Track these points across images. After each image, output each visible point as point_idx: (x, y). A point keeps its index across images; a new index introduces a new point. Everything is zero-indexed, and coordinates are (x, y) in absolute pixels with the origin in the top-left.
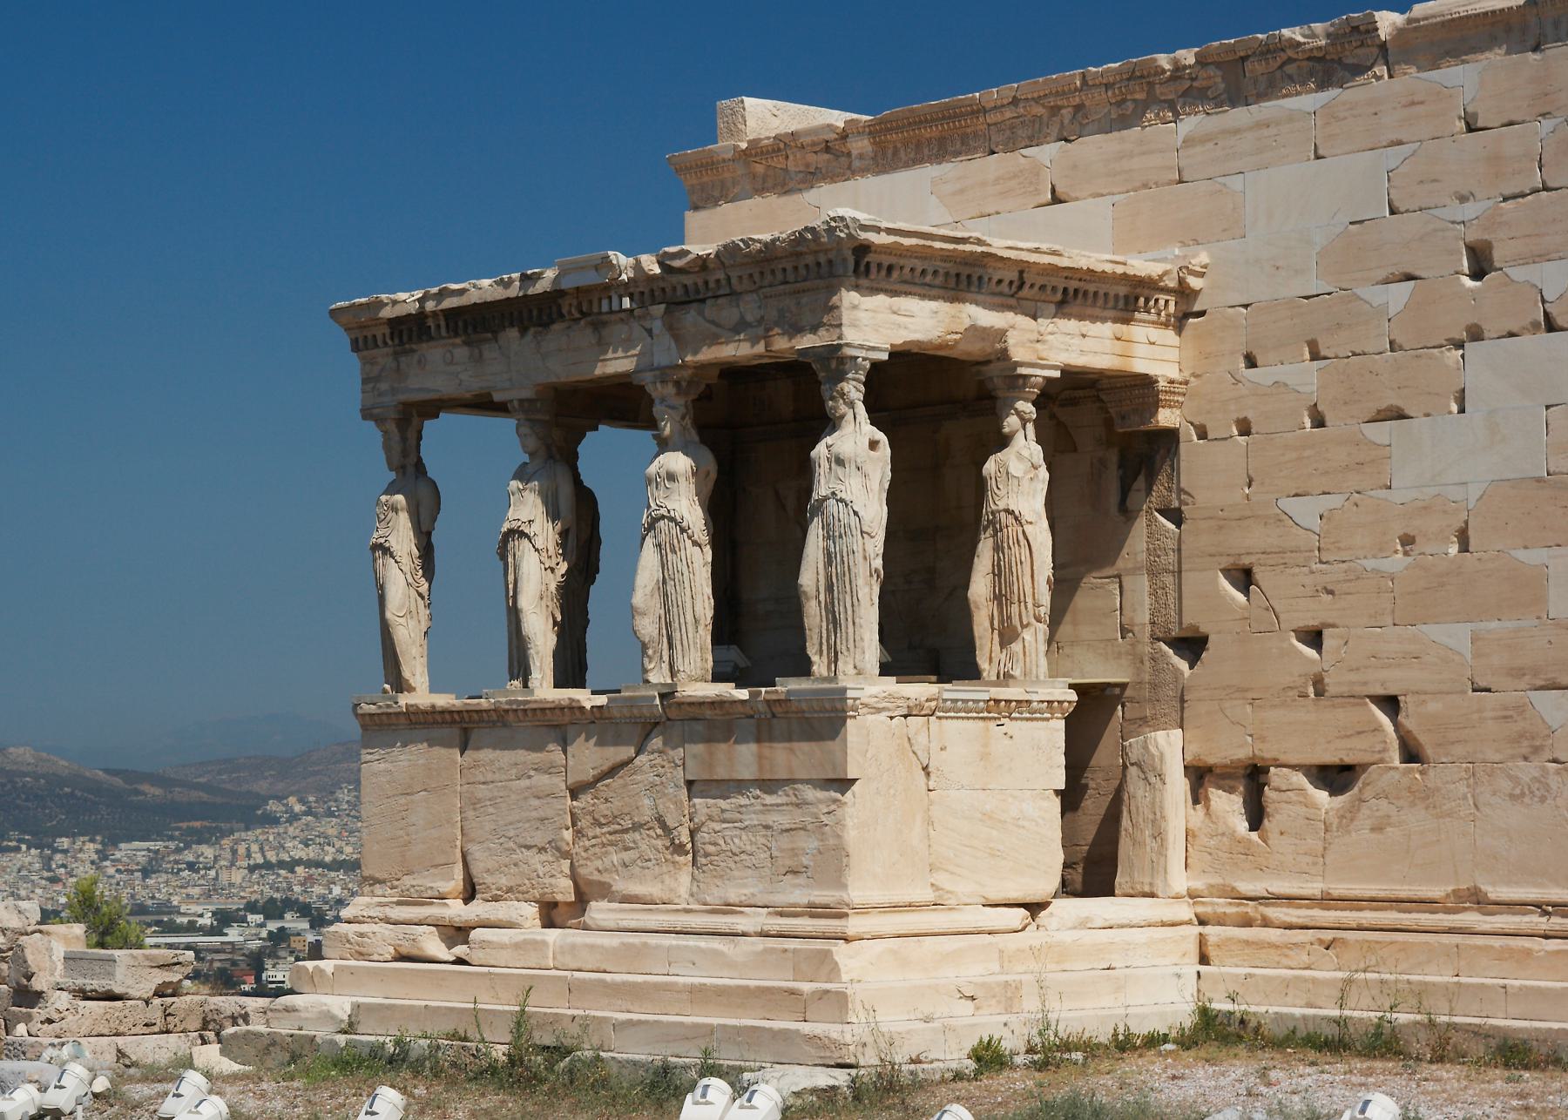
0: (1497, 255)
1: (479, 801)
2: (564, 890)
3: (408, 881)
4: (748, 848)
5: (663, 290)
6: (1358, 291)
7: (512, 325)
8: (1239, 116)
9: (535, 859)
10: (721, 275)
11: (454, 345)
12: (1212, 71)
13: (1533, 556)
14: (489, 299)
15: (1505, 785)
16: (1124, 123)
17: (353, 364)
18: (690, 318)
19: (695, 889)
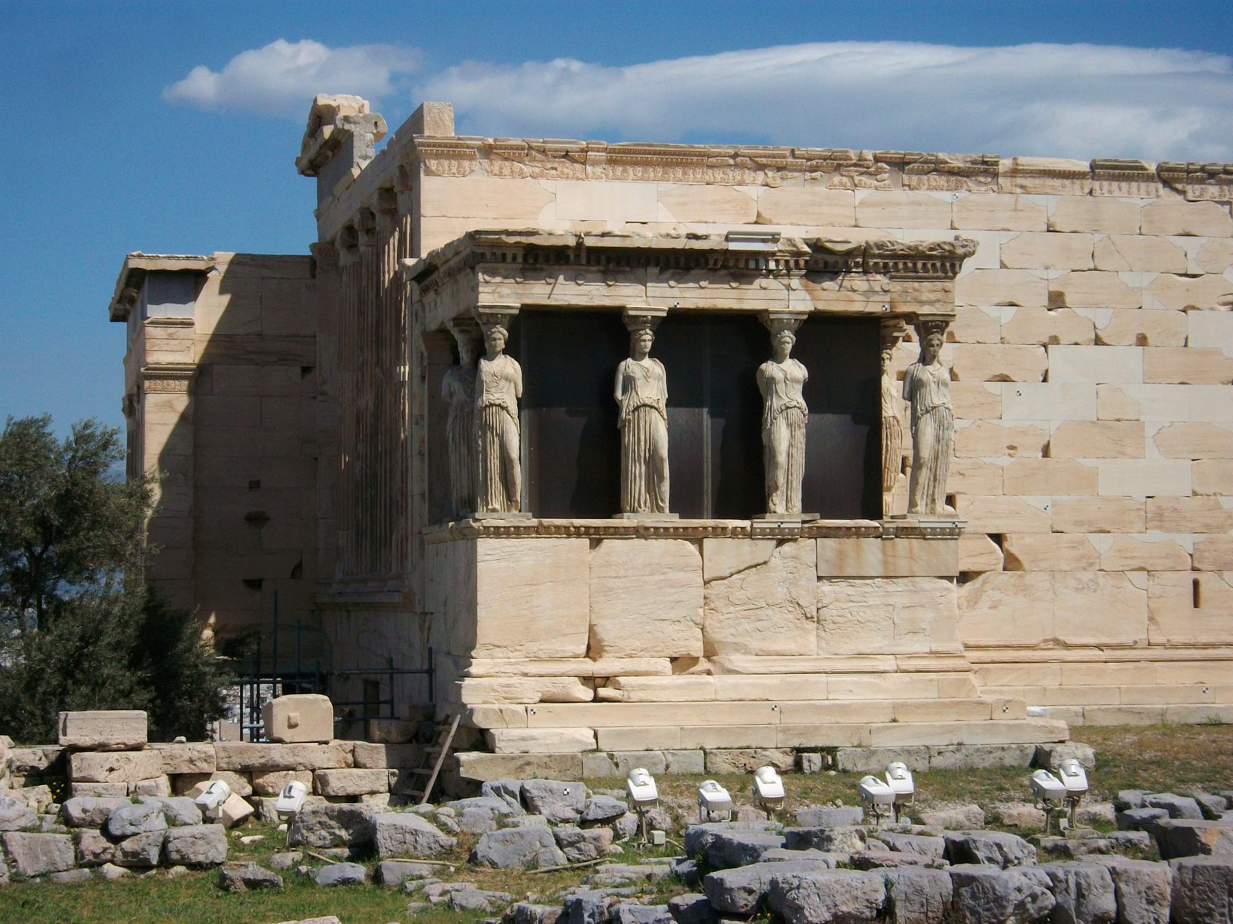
1: (611, 589)
2: (697, 648)
3: (534, 647)
4: (872, 618)
5: (806, 261)
6: (981, 308)
7: (657, 265)
8: (899, 194)
9: (670, 629)
10: (859, 260)
11: (587, 271)
12: (884, 165)
13: (1090, 462)
14: (654, 246)
15: (1073, 583)
19: (823, 644)
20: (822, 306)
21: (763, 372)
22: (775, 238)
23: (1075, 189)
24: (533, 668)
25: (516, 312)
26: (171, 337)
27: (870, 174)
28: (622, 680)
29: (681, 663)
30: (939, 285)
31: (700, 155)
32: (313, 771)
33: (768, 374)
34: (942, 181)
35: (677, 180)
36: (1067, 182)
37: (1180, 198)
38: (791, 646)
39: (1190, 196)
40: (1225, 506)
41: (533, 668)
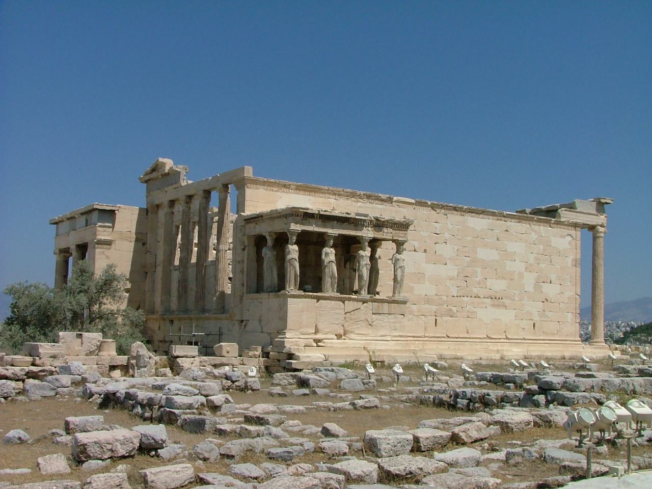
2: (342, 332)
3: (302, 330)
8: (368, 205)
13: (412, 285)
14: (338, 215)
15: (407, 319)
20: (376, 236)
21: (359, 254)
22: (367, 216)
23: (411, 207)
25: (300, 232)
26: (104, 231)
27: (361, 199)
28: (324, 340)
29: (339, 337)
30: (404, 232)
31: (319, 189)
32: (233, 366)
33: (361, 254)
34: (379, 202)
35: (313, 196)
36: (409, 206)
37: (435, 212)
38: (365, 333)
39: (438, 212)
40: (443, 299)
41: (302, 336)
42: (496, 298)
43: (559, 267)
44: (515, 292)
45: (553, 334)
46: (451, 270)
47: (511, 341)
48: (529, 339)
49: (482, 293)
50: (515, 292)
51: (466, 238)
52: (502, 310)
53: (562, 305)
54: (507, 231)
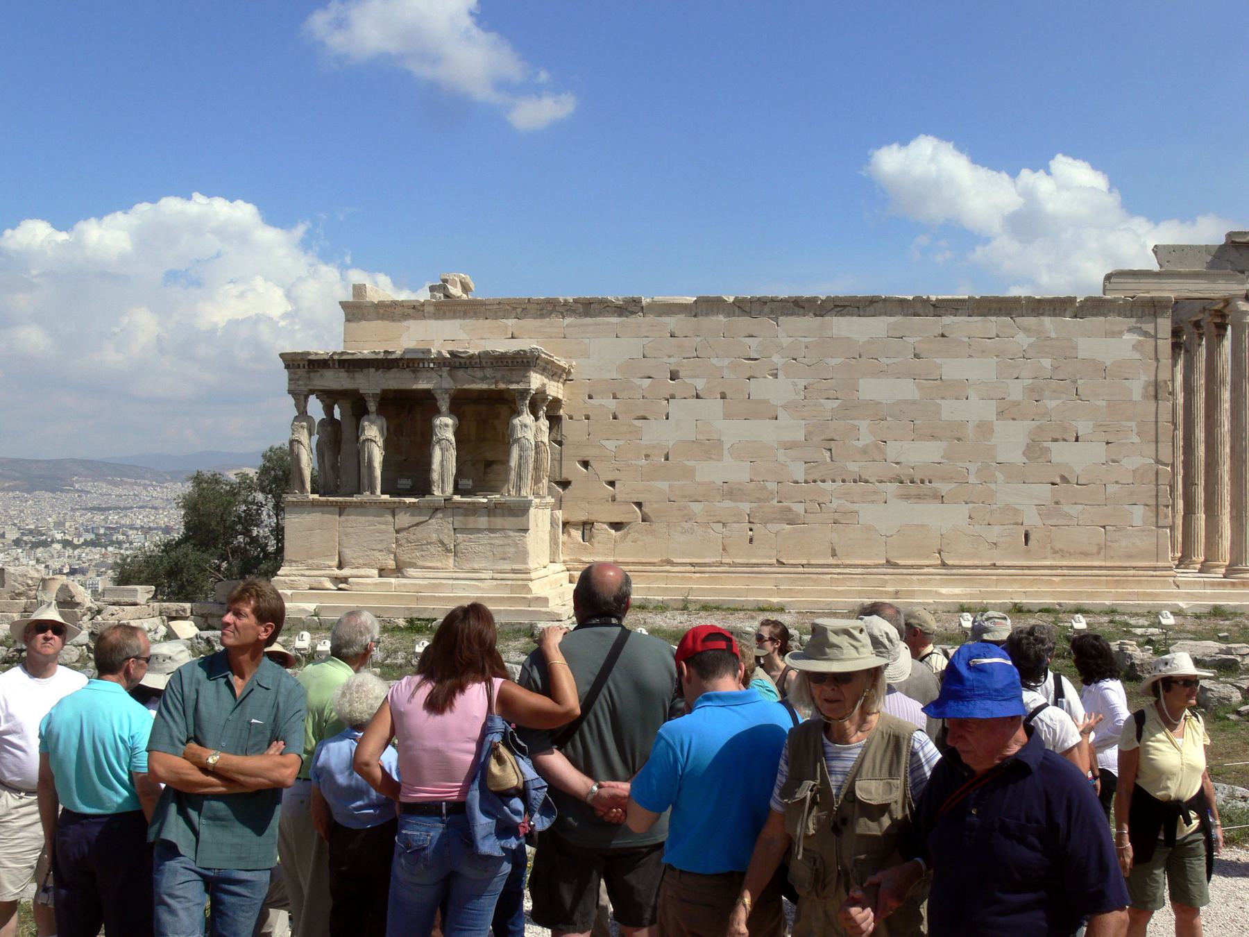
0: (681, 374)
2: (391, 564)
3: (310, 561)
8: (588, 320)
9: (378, 554)
13: (691, 463)
15: (679, 529)
16: (542, 316)
17: (286, 372)
18: (461, 373)
24: (307, 573)
38: (439, 565)
41: (307, 573)
42: (912, 482)
43: (1104, 403)
44: (967, 465)
45: (1086, 555)
46: (791, 429)
47: (954, 571)
48: (1009, 567)
49: (871, 471)
50: (967, 465)
51: (828, 360)
52: (933, 507)
53: (1111, 488)
54: (943, 336)
